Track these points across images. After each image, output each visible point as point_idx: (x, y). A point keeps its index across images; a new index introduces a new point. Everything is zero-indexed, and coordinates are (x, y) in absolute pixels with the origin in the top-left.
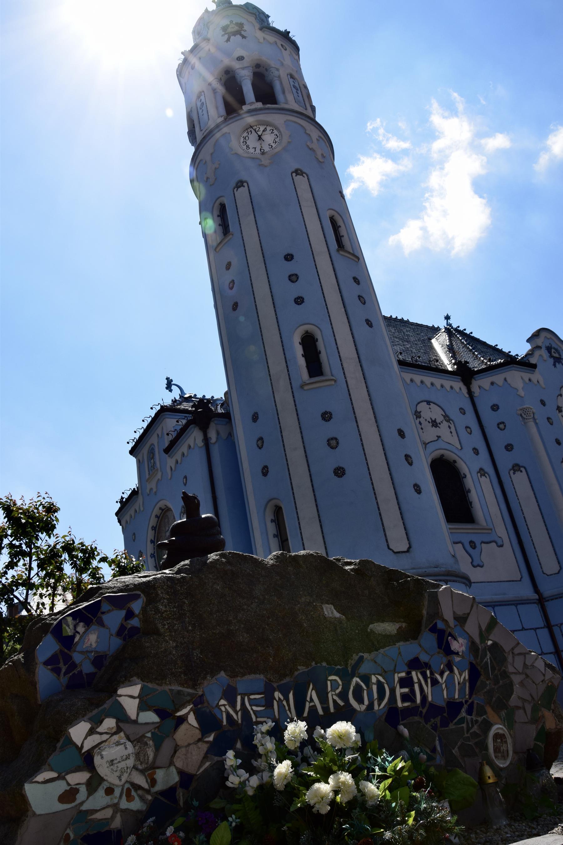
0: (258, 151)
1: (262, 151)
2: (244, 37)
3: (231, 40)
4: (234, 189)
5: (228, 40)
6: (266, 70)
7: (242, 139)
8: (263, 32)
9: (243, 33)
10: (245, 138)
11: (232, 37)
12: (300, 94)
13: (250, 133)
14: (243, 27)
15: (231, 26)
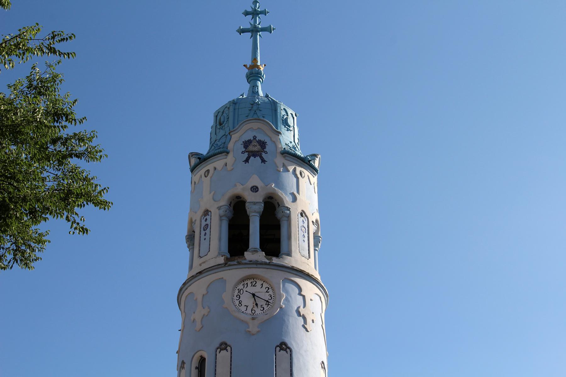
0: (249, 311)
1: (253, 312)
2: (263, 161)
3: (250, 161)
4: (218, 349)
5: (247, 161)
6: (279, 205)
7: (236, 293)
8: (284, 157)
9: (264, 155)
10: (239, 291)
11: (252, 158)
12: (306, 239)
13: (245, 286)
14: (265, 148)
15: (253, 144)
